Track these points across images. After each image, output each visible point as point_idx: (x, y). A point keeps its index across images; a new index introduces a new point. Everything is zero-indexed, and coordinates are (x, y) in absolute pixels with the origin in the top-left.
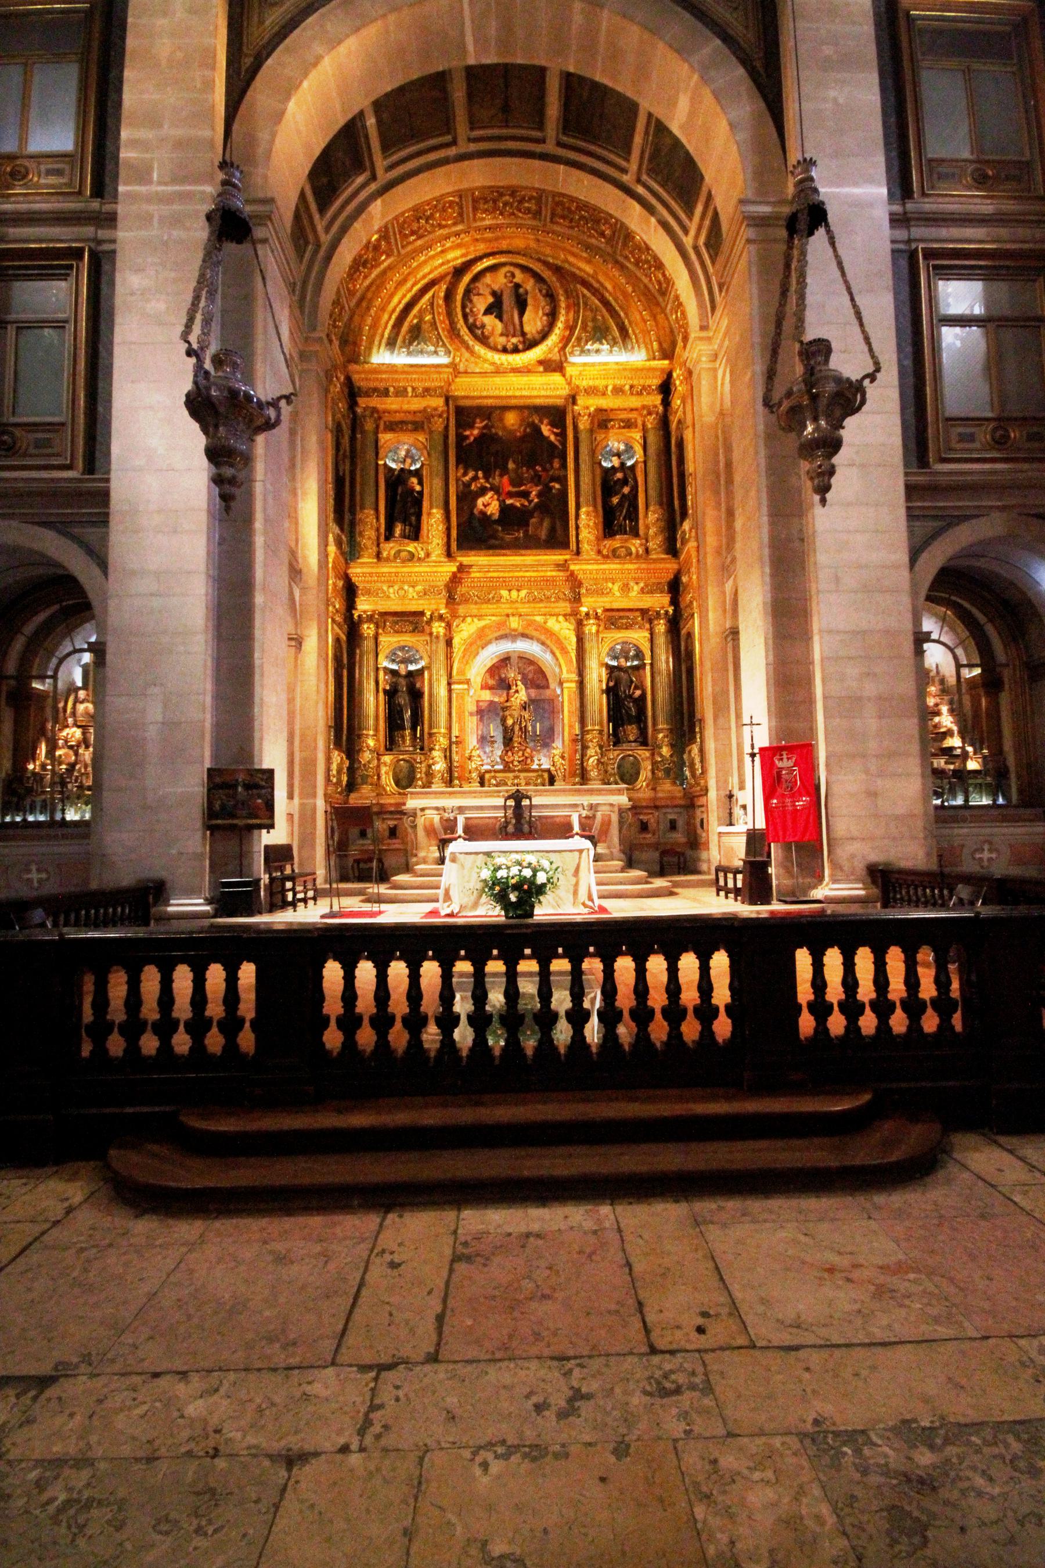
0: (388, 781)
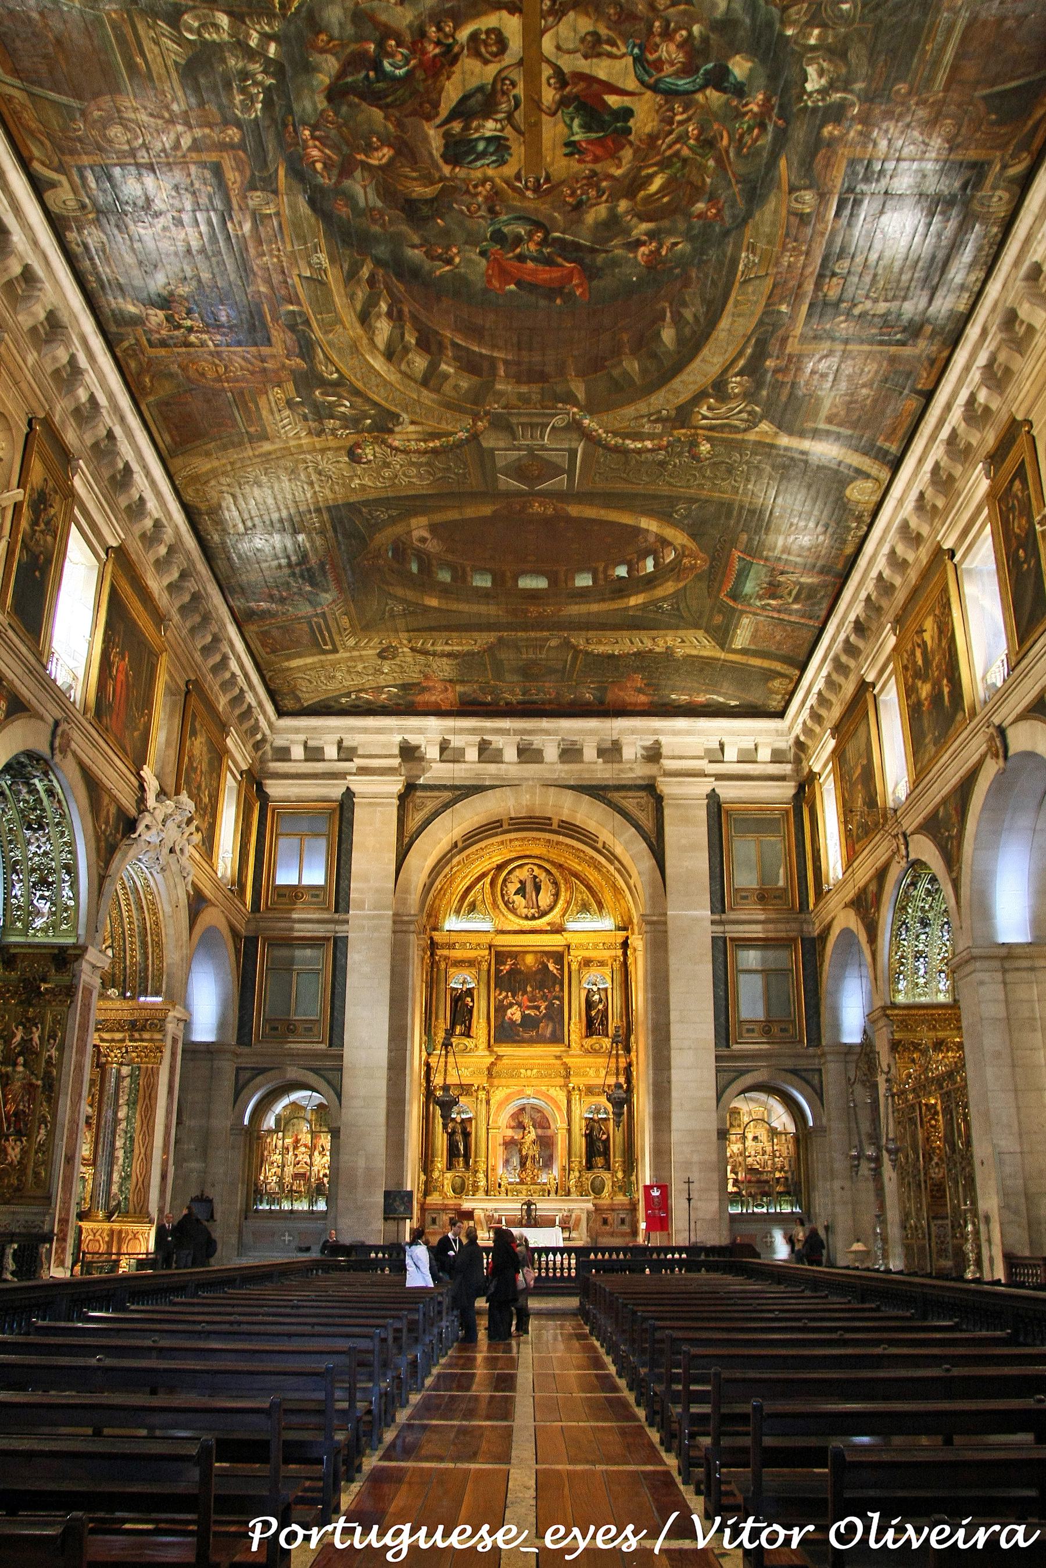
0: (448, 1189)
